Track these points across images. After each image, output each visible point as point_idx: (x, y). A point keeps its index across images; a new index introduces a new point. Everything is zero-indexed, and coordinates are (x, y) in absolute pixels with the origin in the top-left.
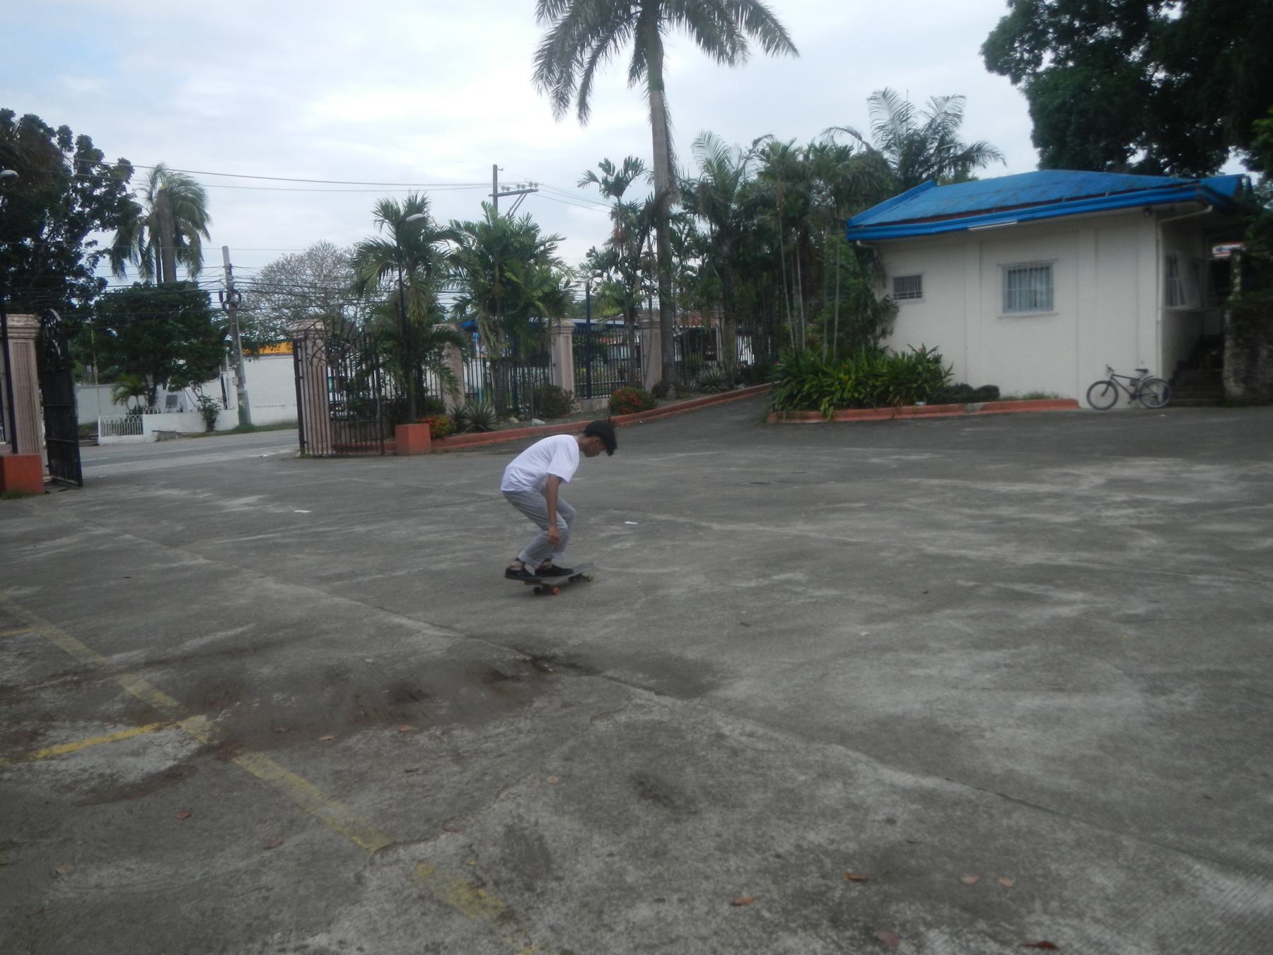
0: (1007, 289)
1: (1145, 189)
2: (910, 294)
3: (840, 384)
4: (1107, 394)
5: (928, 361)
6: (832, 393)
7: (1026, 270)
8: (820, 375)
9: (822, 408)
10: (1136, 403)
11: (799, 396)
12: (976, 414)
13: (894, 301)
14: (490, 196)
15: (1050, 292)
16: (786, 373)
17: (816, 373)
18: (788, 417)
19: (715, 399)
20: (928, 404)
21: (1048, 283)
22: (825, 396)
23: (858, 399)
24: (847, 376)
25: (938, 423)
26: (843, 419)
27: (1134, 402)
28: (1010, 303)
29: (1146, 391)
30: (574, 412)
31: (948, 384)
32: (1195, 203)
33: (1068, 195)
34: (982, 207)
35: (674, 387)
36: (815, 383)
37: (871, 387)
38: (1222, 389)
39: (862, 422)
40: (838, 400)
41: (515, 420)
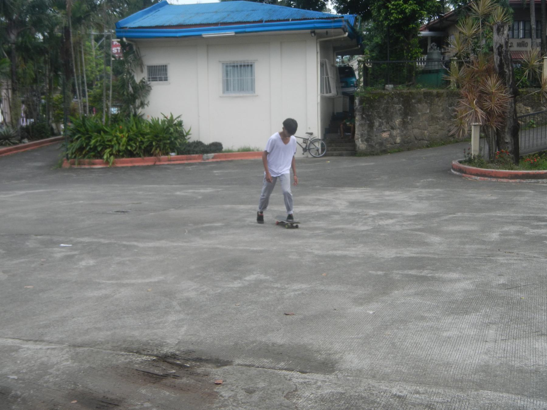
0: (225, 78)
1: (313, 19)
2: (159, 78)
3: (117, 140)
6: (112, 146)
7: (237, 66)
8: (102, 133)
9: (105, 157)
10: (307, 154)
11: (88, 148)
12: (210, 161)
13: (148, 83)
15: (253, 81)
16: (76, 131)
17: (99, 132)
18: (80, 164)
20: (178, 154)
22: (106, 148)
23: (130, 151)
25: (190, 168)
26: (119, 165)
27: (305, 153)
28: (227, 87)
29: (312, 146)
31: (188, 141)
32: (341, 30)
33: (264, 20)
34: (211, 22)
36: (99, 139)
37: (139, 142)
38: (354, 145)
39: (133, 167)
40: (116, 152)
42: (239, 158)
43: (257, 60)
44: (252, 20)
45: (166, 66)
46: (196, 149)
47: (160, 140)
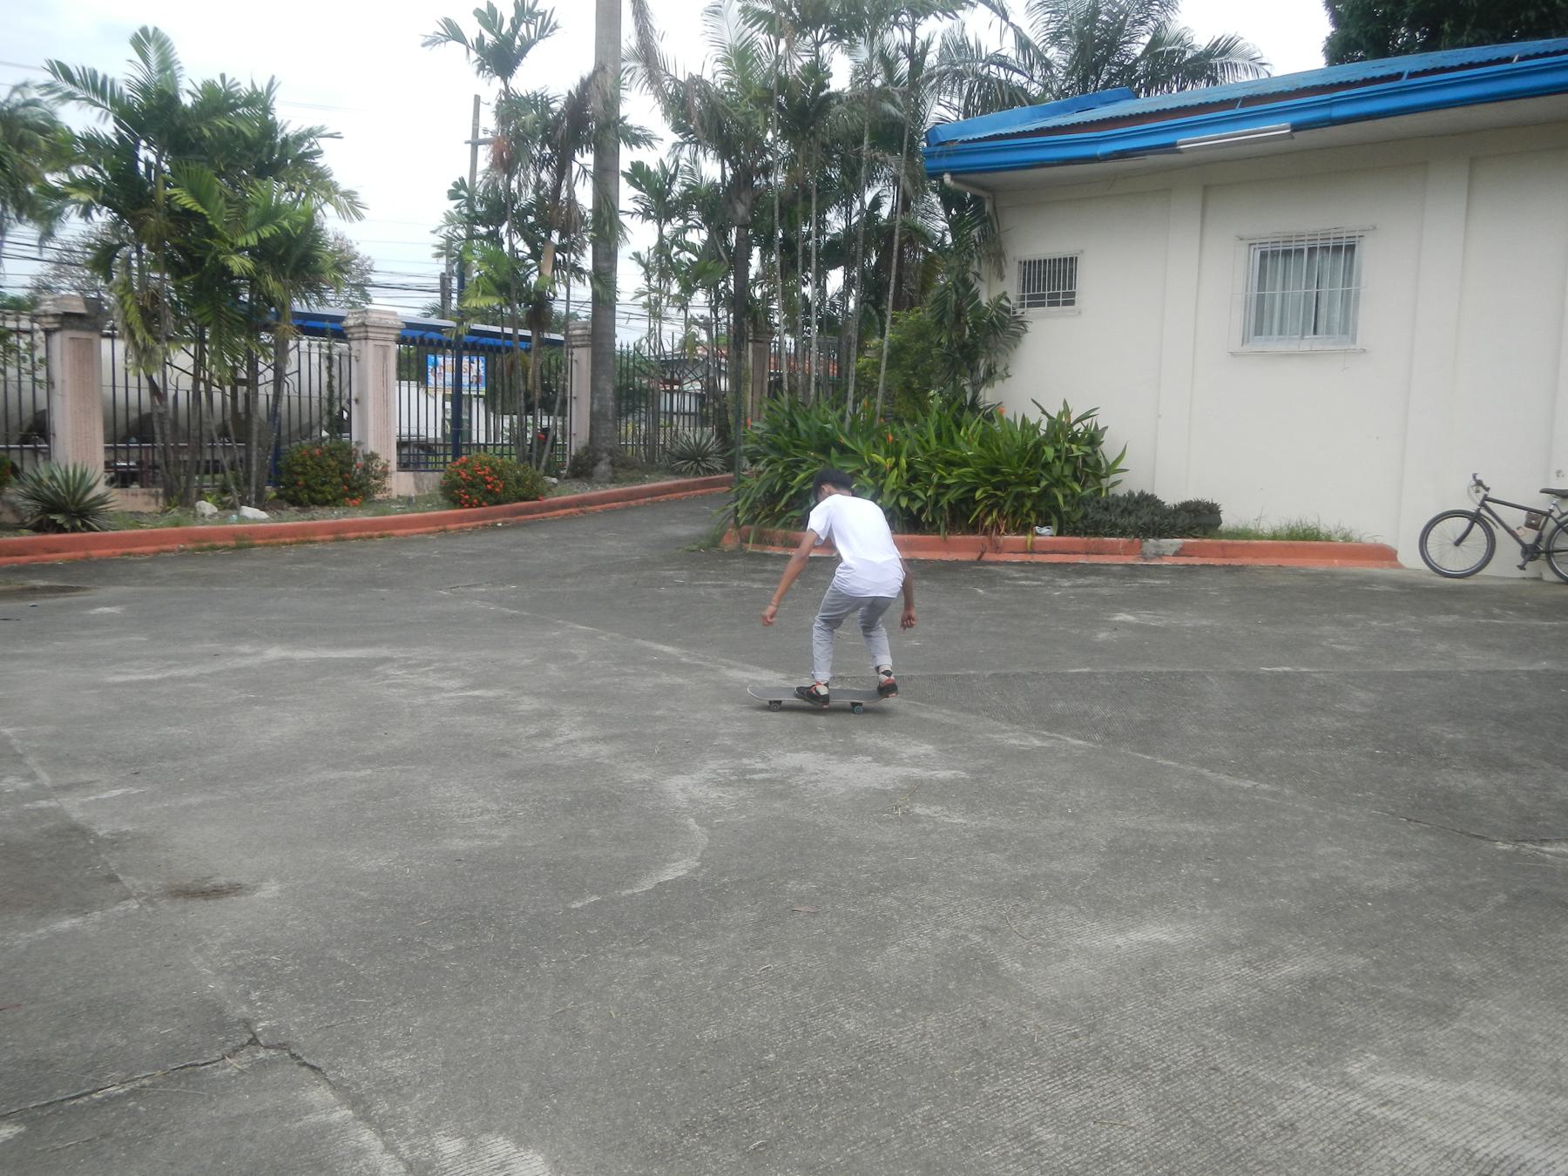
0: (1255, 292)
3: (872, 475)
4: (1463, 543)
5: (1074, 439)
7: (1300, 252)
8: (833, 450)
14: (467, 142)
15: (1349, 301)
17: (824, 449)
18: (760, 540)
19: (686, 487)
20: (1059, 533)
21: (1348, 280)
24: (891, 461)
27: (1529, 565)
28: (1261, 320)
30: (378, 496)
31: (1111, 491)
35: (608, 460)
41: (207, 507)
42: (1274, 562)
43: (1375, 228)
44: (1361, 79)
45: (1072, 261)
46: (1122, 521)
47: (1003, 485)
